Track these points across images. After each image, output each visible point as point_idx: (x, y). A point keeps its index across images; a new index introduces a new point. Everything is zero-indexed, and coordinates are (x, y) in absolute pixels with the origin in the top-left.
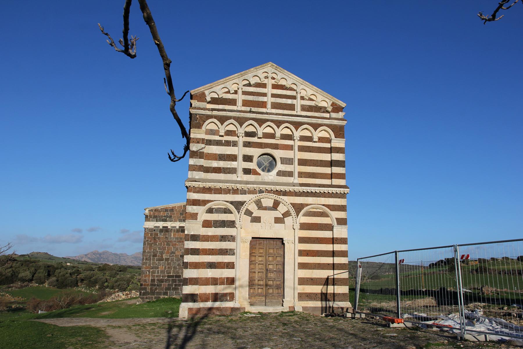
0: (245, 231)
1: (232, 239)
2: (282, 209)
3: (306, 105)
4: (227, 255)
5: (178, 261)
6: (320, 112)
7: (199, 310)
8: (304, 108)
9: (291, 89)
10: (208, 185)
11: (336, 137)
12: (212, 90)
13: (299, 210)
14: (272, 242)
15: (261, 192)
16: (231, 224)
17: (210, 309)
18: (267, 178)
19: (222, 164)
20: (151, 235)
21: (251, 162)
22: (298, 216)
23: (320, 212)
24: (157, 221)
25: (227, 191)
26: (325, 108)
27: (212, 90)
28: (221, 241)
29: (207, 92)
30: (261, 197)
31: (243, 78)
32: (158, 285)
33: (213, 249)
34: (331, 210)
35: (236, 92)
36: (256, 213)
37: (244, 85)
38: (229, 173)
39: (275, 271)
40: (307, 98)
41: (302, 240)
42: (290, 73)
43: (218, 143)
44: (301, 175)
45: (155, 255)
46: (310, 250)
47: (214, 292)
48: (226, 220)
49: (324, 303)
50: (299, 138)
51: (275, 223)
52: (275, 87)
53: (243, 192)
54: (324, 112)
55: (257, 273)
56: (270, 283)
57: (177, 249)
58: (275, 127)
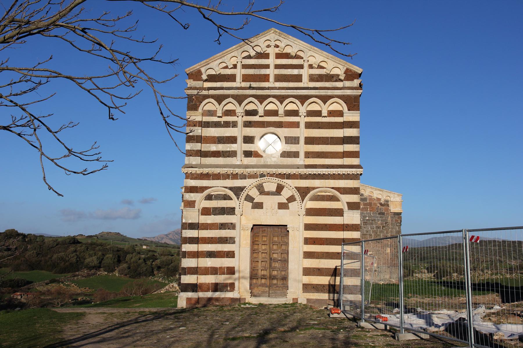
0: (246, 218)
1: (232, 226)
2: (286, 193)
3: (315, 75)
4: (226, 243)
6: (331, 81)
7: (198, 300)
8: (313, 78)
9: (297, 57)
10: (206, 171)
11: (349, 110)
12: (208, 67)
13: (304, 194)
14: (276, 229)
15: (262, 175)
16: (231, 211)
17: (210, 299)
18: (270, 160)
19: (221, 147)
21: (252, 143)
22: (303, 201)
23: (329, 196)
25: (226, 177)
26: (338, 75)
27: (208, 67)
28: (220, 229)
29: (203, 70)
30: (263, 181)
31: (242, 50)
33: (212, 238)
34: (341, 193)
35: (235, 67)
36: (258, 198)
37: (244, 58)
38: (228, 157)
39: (279, 260)
40: (316, 67)
41: (308, 227)
42: (295, 39)
43: (217, 125)
44: (308, 155)
46: (317, 238)
47: (214, 282)
48: (225, 206)
49: (331, 295)
50: (305, 114)
51: (279, 208)
52: (279, 56)
53: (243, 177)
54: (336, 81)
55: (260, 262)
56: (275, 273)
58: (278, 103)
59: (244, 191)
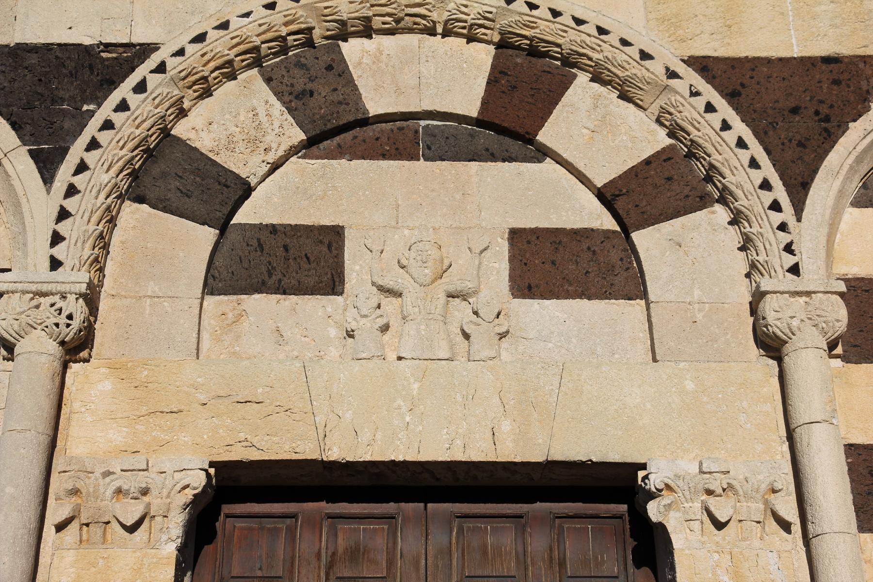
22: (799, 189)
59: (124, 90)
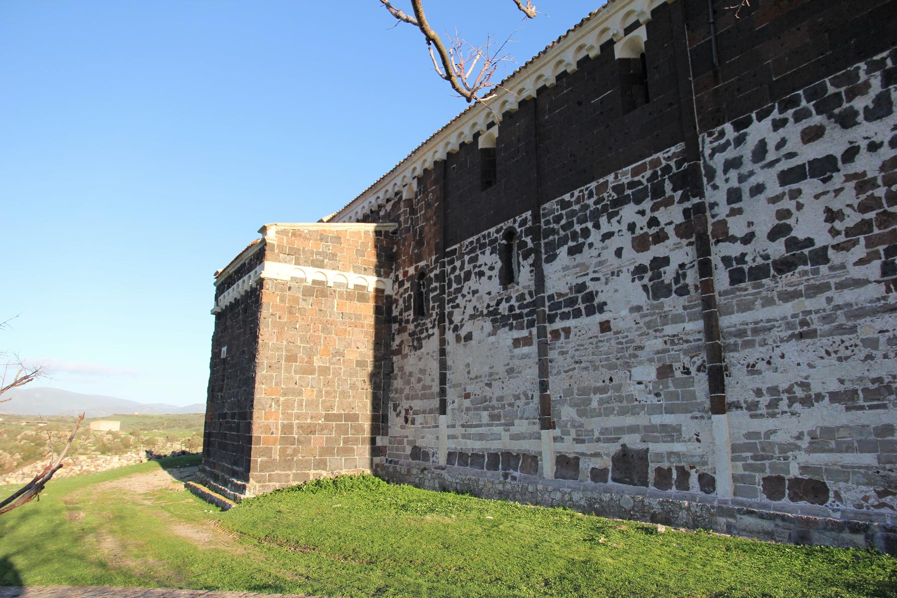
5: (351, 375)
20: (282, 300)
24: (297, 263)
32: (299, 442)
45: (291, 358)
57: (349, 344)
